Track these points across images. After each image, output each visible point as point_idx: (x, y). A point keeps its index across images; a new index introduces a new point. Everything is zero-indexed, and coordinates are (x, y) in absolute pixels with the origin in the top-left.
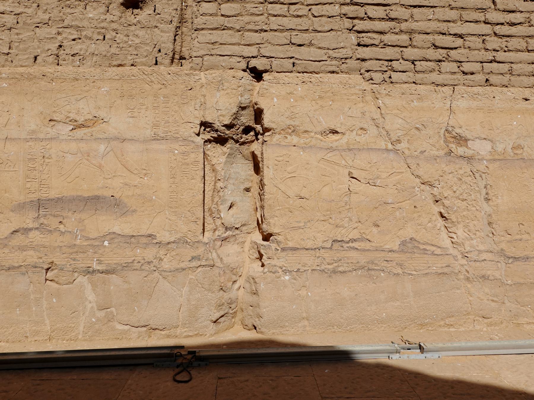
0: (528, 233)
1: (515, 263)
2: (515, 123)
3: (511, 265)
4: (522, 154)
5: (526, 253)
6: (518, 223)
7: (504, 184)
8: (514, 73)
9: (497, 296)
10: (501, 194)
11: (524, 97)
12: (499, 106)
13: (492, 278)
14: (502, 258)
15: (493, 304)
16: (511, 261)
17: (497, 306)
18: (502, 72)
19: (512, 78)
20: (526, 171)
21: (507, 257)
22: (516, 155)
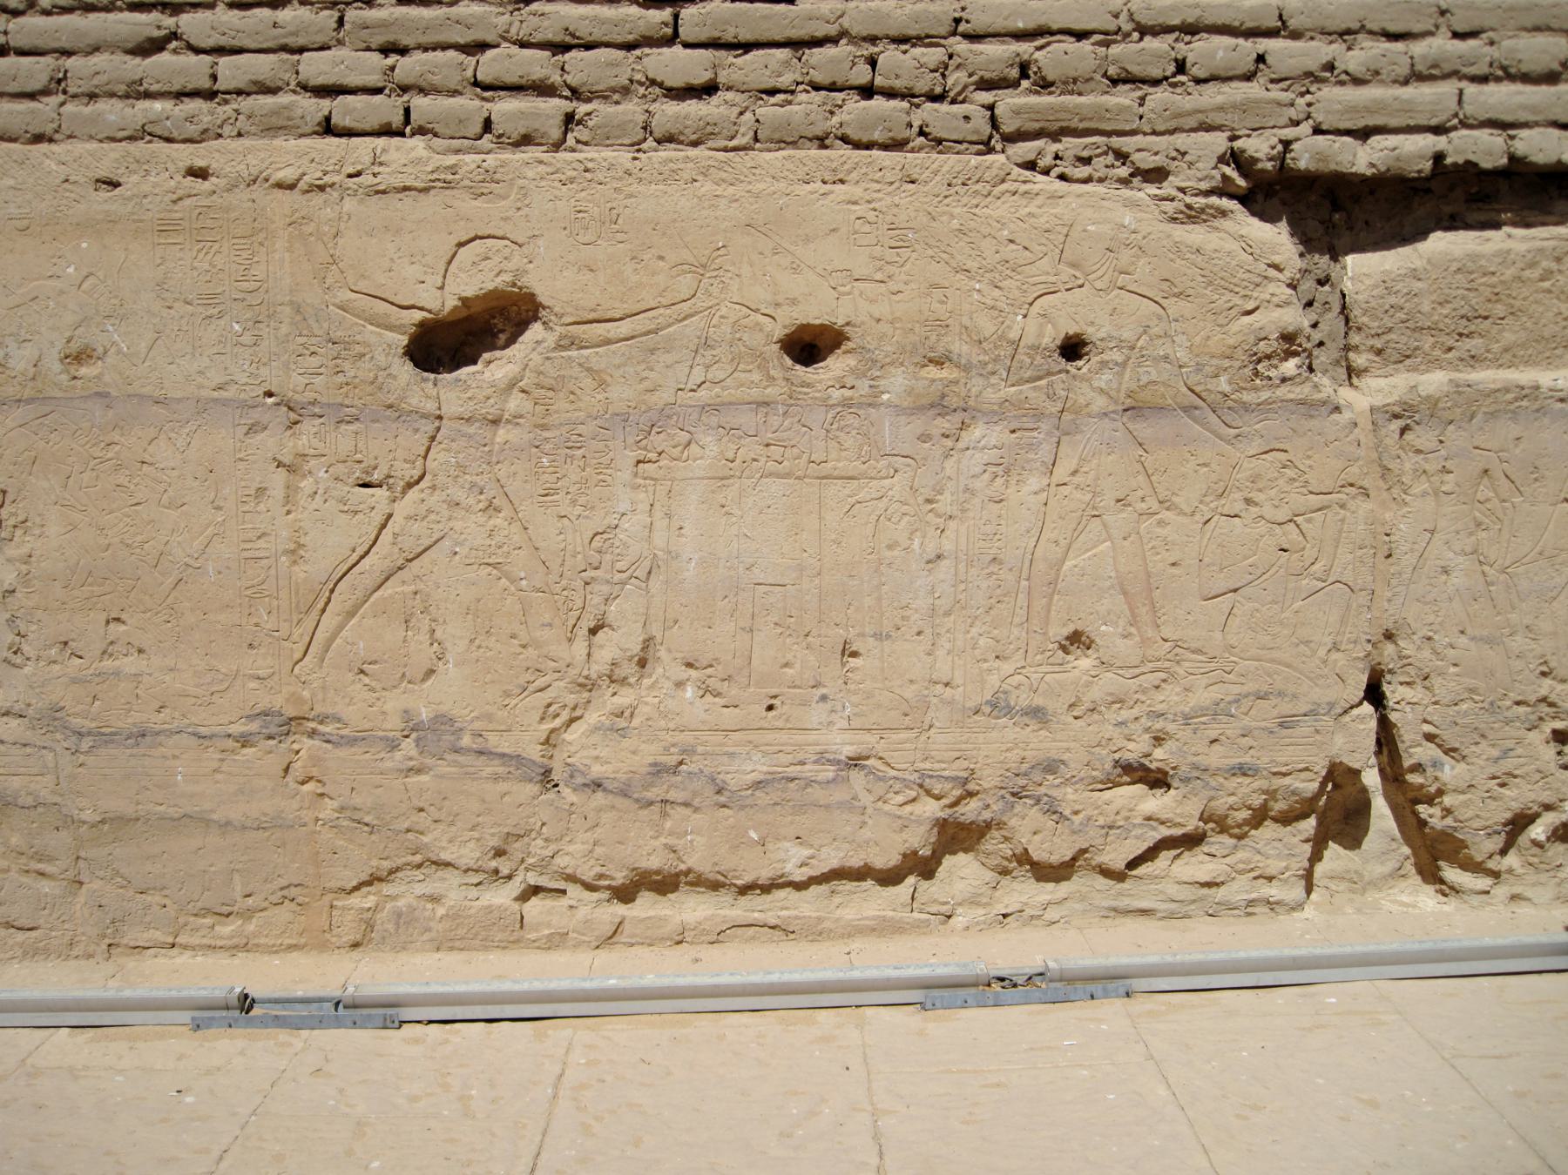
0: (140, 651)
1: (103, 751)
2: (71, 270)
3: (90, 760)
4: (98, 377)
5: (136, 717)
6: (103, 617)
7: (45, 484)
8: (72, 90)
9: (51, 859)
10: (38, 520)
11: (103, 173)
12: (12, 210)
13: (30, 801)
14: (58, 736)
15: (46, 887)
16: (86, 744)
17: (57, 891)
18: (28, 89)
19: (70, 108)
20: (117, 438)
21: (74, 732)
22: (79, 383)
